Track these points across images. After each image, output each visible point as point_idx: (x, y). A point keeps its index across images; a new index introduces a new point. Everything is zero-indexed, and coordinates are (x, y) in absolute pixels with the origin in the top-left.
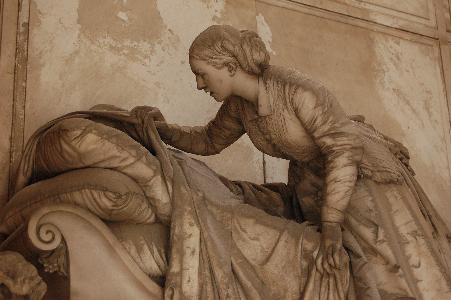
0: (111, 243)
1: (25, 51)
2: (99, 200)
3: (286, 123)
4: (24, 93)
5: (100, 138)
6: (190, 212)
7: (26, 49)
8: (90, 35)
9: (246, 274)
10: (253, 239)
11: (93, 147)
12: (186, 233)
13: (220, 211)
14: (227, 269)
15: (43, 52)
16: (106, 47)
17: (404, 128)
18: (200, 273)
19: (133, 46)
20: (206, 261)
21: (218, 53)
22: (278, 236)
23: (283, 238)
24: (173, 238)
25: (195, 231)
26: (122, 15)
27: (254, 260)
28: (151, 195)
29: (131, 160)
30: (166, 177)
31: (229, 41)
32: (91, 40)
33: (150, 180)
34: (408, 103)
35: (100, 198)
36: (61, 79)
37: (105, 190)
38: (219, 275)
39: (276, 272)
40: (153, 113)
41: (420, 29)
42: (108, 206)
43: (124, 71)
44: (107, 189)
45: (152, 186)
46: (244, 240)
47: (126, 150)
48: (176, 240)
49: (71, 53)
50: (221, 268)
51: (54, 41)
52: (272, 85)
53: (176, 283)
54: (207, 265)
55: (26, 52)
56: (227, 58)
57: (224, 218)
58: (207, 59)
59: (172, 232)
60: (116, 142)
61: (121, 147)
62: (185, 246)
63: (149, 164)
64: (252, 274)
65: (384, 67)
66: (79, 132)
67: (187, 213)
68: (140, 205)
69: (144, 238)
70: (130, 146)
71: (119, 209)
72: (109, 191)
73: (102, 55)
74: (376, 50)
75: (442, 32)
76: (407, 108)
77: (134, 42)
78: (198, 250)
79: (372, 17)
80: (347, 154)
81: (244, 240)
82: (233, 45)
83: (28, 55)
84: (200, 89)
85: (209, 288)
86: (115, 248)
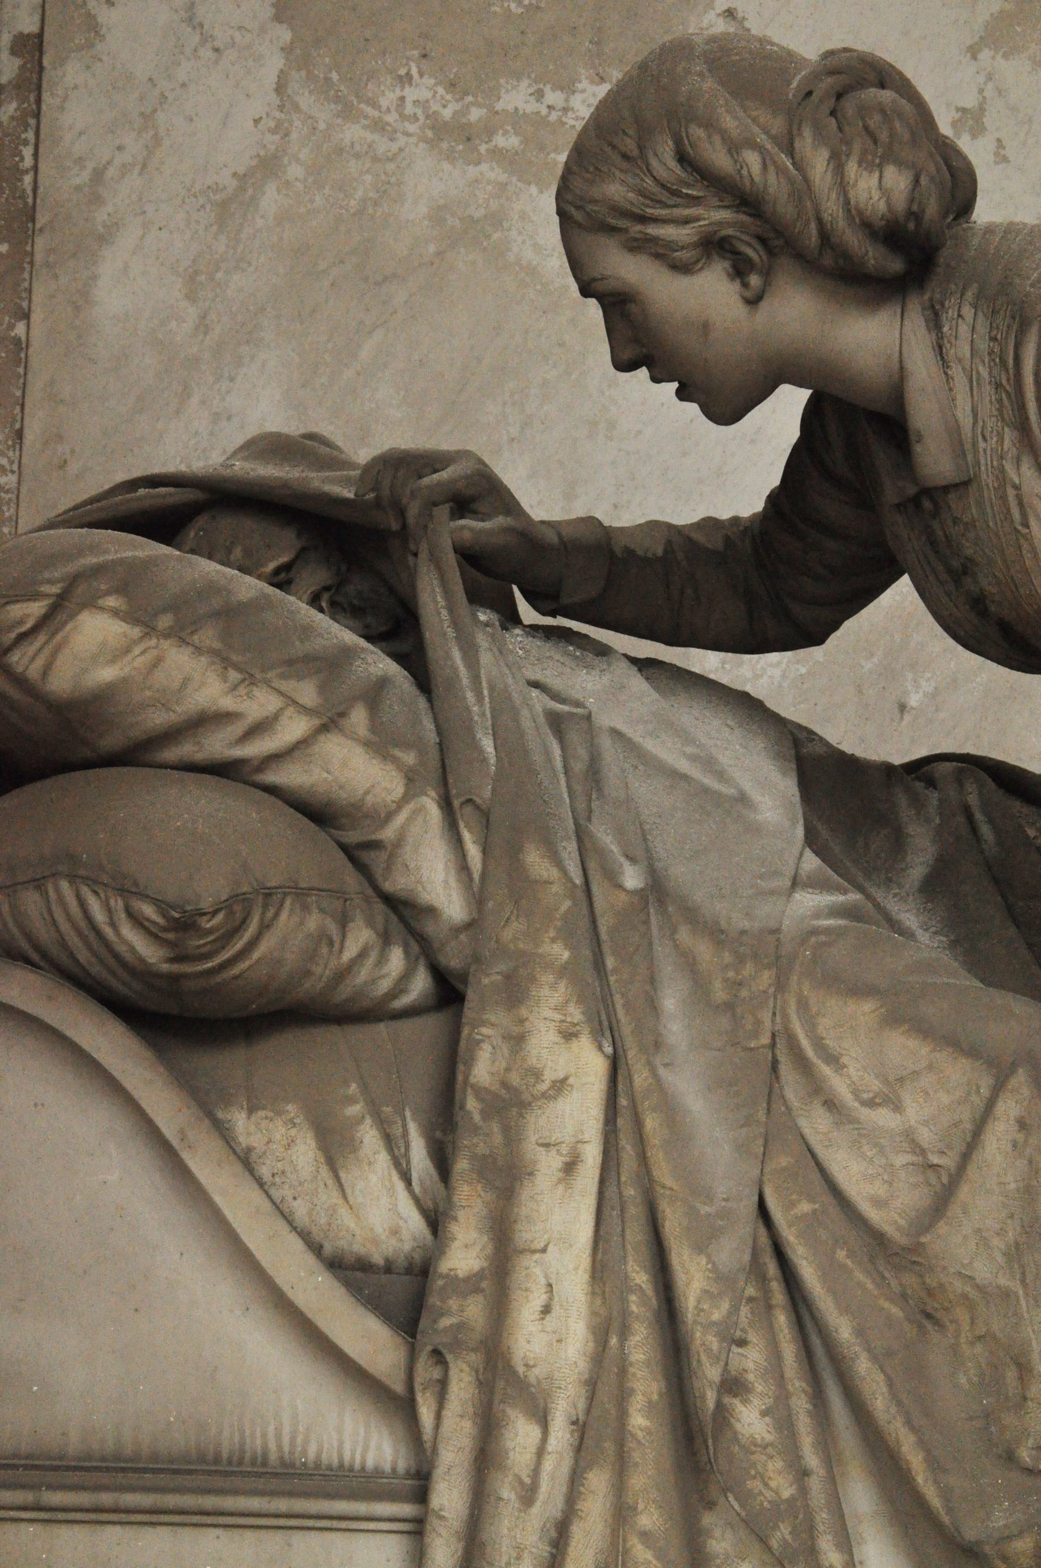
0: (169, 1132)
1: (27, 172)
2: (108, 931)
3: (1033, 522)
4: (21, 370)
5: (136, 632)
6: (563, 971)
7: (28, 162)
8: (335, 76)
9: (829, 1271)
10: (871, 1104)
11: (107, 674)
12: (537, 1074)
13: (728, 957)
14: (733, 1249)
15: (111, 172)
16: (412, 128)
18: (602, 1270)
19: (544, 111)
20: (635, 1211)
21: (664, 196)
22: (985, 1092)
23: (1008, 1108)
24: (462, 1107)
25: (587, 1064)
27: (879, 1203)
28: (397, 883)
29: (294, 728)
30: (456, 803)
31: (710, 125)
32: (337, 99)
33: (390, 816)
35: (113, 924)
36: (191, 297)
37: (128, 889)
38: (687, 1285)
39: (983, 1271)
40: (453, 481)
42: (153, 960)
43: (496, 236)
44: (136, 884)
45: (399, 842)
46: (831, 1104)
47: (268, 683)
48: (477, 1117)
49: (241, 170)
50: (700, 1248)
51: (161, 117)
52: (967, 329)
53: (461, 1326)
54: (636, 1234)
55: (28, 179)
56: (717, 216)
57: (744, 993)
58: (622, 223)
59: (460, 1078)
60: (217, 645)
61: (237, 668)
62: (532, 1139)
63: (381, 743)
64: (860, 1276)
66: (36, 609)
67: (551, 978)
68: (331, 943)
69: (364, 1087)
70: (290, 662)
71: (210, 972)
72: (145, 897)
73: (391, 167)
77: (547, 89)
78: (592, 1155)
81: (831, 1104)
82: (734, 148)
83: (41, 190)
84: (624, 365)
85: (641, 1347)
86: (186, 1156)
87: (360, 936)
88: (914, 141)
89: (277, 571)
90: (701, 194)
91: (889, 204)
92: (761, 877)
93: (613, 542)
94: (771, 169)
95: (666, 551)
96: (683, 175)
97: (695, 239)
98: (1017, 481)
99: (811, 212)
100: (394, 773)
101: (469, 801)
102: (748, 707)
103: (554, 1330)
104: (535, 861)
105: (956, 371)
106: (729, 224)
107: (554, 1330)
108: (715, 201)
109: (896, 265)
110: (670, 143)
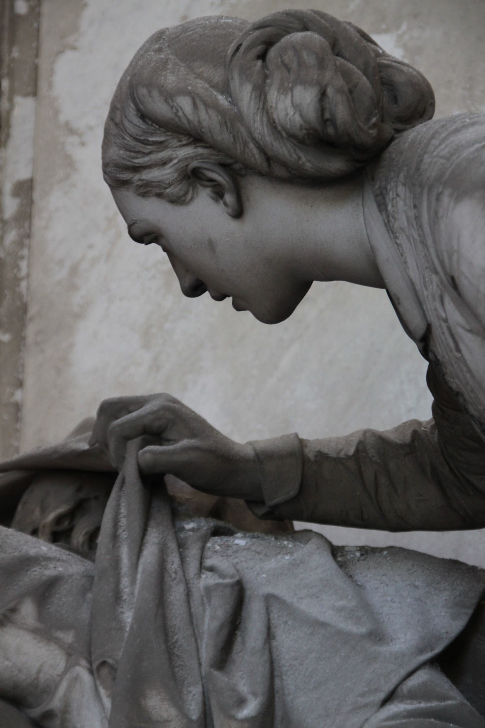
1: (22, 279)
3: (462, 347)
21: (140, 147)
36: (146, 345)
45: (66, 710)
56: (183, 153)
58: (126, 176)
88: (321, 64)
89: (59, 520)
90: (162, 139)
91: (302, 116)
92: (363, 695)
93: (307, 451)
94: (202, 107)
95: (357, 450)
96: (144, 126)
97: (176, 175)
98: (444, 315)
99: (245, 134)
100: (57, 652)
101: (104, 663)
105: (402, 240)
106: (192, 158)
108: (175, 143)
109: (335, 165)
110: (132, 105)
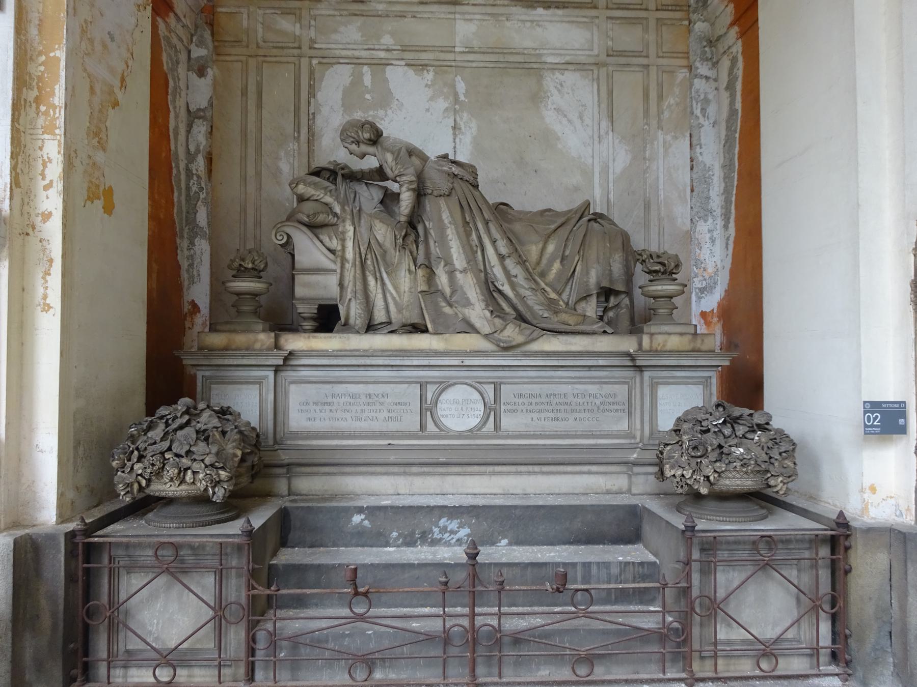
14: (366, 246)
17: (560, 134)
25: (352, 228)
26: (368, 96)
34: (565, 116)
41: (583, 59)
63: (331, 196)
65: (549, 94)
74: (544, 83)
75: (603, 57)
76: (564, 121)
79: (545, 59)
80: (406, 186)
87: (331, 217)
102: (382, 187)
103: (350, 254)
104: (346, 208)
107: (350, 254)
